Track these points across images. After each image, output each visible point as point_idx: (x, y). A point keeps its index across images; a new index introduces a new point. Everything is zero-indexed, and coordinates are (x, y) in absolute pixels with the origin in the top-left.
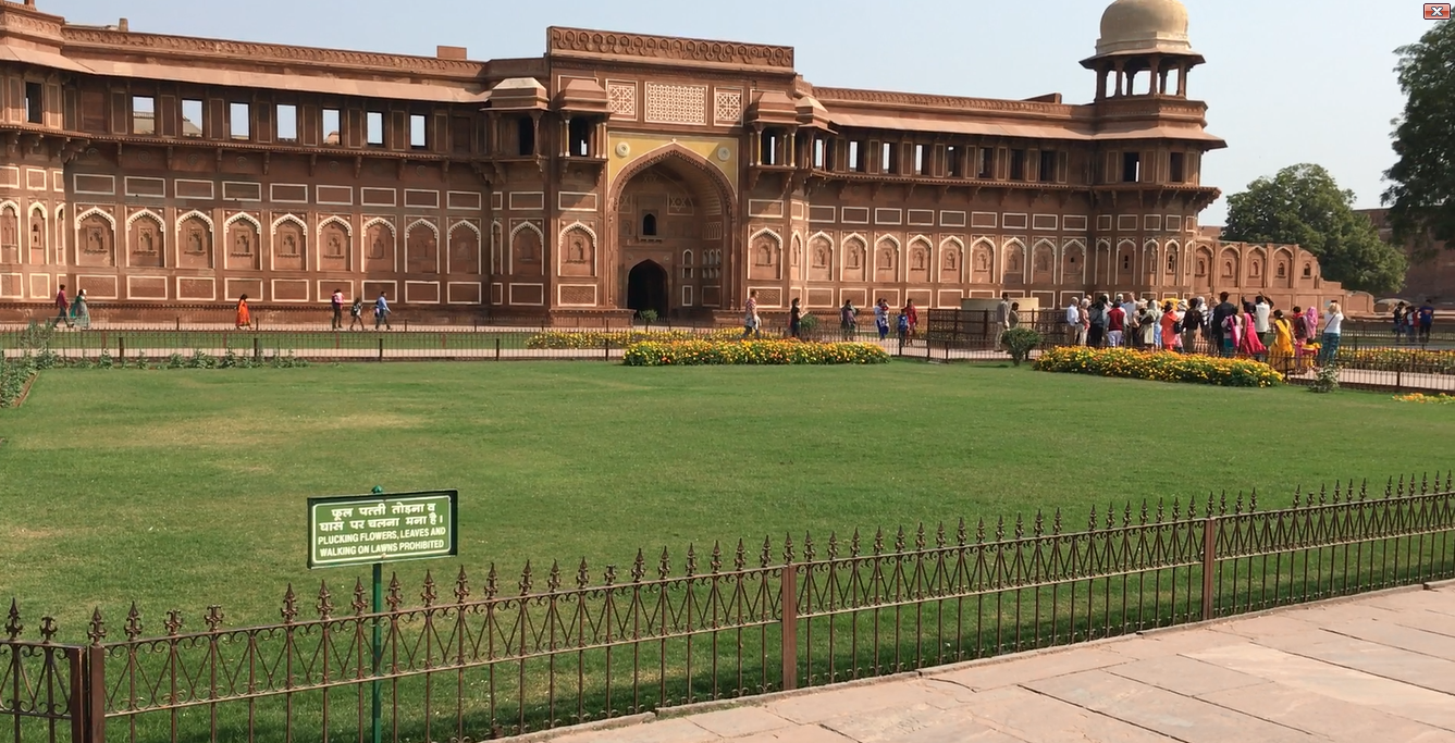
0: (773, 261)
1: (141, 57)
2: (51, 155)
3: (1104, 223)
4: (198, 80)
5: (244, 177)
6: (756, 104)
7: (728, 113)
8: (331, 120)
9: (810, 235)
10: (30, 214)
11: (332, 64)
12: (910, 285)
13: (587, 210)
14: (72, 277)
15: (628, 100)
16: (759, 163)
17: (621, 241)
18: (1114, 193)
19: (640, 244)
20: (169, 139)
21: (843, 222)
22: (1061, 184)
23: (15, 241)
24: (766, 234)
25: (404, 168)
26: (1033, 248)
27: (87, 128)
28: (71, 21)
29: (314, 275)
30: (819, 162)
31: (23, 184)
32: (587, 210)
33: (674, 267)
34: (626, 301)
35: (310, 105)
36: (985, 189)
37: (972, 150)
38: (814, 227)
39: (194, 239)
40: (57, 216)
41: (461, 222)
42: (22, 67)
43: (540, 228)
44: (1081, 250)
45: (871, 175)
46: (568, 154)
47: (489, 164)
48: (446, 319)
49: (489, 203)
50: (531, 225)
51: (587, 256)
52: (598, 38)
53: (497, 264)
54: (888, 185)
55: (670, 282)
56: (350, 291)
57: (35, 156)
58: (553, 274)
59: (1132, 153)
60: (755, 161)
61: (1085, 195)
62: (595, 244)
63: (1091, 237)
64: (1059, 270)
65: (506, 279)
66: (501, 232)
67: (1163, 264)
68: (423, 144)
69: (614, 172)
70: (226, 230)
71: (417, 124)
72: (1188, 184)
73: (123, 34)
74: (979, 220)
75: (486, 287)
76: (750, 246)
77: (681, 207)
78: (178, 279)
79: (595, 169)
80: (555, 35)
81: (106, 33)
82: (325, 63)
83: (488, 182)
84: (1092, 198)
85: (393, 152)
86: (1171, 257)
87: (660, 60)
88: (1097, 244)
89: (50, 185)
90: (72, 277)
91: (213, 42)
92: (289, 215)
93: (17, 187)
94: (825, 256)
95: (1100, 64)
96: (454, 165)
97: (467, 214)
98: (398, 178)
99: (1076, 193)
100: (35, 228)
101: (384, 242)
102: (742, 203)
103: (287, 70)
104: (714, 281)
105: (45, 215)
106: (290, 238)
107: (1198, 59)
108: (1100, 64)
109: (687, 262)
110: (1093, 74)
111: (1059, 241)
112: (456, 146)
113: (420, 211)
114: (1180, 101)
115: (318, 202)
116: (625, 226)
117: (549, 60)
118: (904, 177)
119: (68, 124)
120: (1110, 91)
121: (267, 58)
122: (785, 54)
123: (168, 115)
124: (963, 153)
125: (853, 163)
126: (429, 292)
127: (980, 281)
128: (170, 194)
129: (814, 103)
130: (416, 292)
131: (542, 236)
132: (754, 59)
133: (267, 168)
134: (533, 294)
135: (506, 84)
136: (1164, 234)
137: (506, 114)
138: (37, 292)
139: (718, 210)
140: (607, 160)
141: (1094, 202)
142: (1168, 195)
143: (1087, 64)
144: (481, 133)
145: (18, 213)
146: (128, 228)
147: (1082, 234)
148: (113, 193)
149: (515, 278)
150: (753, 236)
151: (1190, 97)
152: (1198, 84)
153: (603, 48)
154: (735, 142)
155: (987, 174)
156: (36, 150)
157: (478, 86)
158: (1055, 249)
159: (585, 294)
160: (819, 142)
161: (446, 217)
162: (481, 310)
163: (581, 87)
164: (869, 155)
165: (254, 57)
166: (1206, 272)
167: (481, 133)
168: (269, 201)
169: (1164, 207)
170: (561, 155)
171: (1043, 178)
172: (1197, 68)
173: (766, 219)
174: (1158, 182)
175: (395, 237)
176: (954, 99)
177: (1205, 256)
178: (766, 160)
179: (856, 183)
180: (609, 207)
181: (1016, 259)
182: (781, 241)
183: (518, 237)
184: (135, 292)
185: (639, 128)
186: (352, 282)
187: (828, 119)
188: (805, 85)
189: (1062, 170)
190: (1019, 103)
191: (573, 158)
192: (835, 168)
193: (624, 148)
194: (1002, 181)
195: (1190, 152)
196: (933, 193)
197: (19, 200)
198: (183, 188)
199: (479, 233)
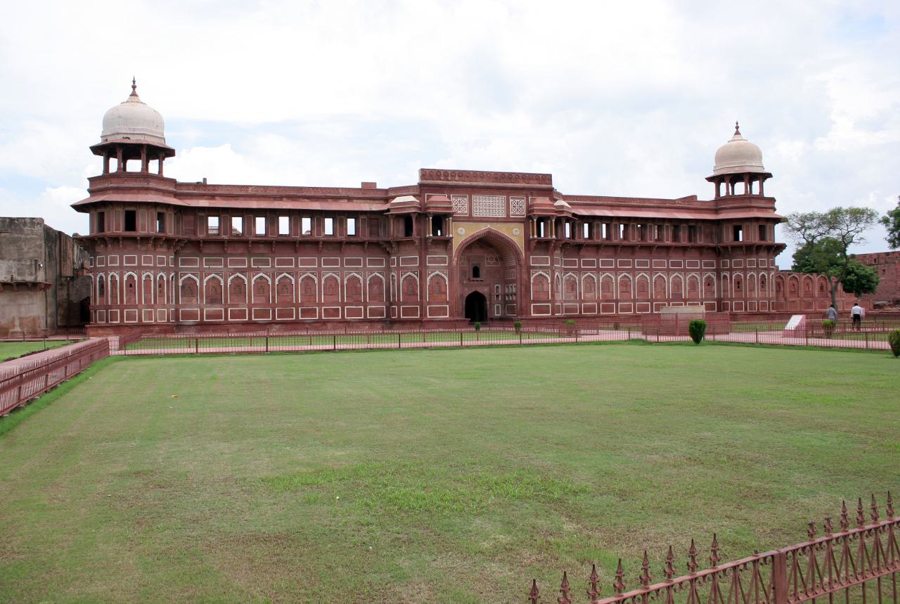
1: (213, 197)
2: (169, 248)
4: (240, 206)
5: (262, 255)
6: (533, 205)
8: (306, 224)
9: (564, 275)
10: (158, 279)
11: (307, 194)
12: (621, 301)
14: (177, 311)
16: (536, 236)
17: (461, 282)
18: (730, 249)
19: (472, 283)
20: (225, 237)
21: (582, 267)
22: (701, 242)
23: (150, 293)
24: (541, 275)
25: (343, 246)
26: (687, 278)
27: (186, 233)
28: (180, 180)
29: (297, 305)
30: (568, 235)
31: (155, 264)
33: (490, 295)
34: (464, 313)
35: (296, 215)
36: (659, 247)
37: (651, 226)
38: (566, 271)
39: (238, 289)
40: (171, 279)
41: (374, 274)
42: (156, 205)
43: (417, 275)
44: (713, 279)
45: (596, 241)
46: (431, 235)
47: (388, 242)
49: (388, 262)
50: (413, 275)
51: (443, 290)
52: (446, 174)
53: (394, 296)
54: (606, 246)
55: (488, 303)
57: (161, 250)
58: (424, 300)
59: (737, 225)
60: (533, 235)
61: (714, 249)
62: (447, 283)
63: (718, 271)
64: (702, 291)
65: (398, 304)
67: (757, 285)
68: (354, 233)
69: (456, 244)
70: (253, 283)
71: (351, 223)
72: (769, 242)
73: (202, 185)
74: (656, 264)
76: (532, 281)
79: (446, 243)
80: (425, 173)
81: (198, 185)
82: (304, 194)
83: (388, 253)
84: (717, 250)
85: (339, 238)
86: (763, 282)
87: (481, 184)
89: (168, 263)
90: (177, 311)
91: (247, 187)
92: (285, 274)
93: (152, 265)
94: (572, 286)
95: (717, 180)
96: (371, 244)
97: (378, 270)
98: (341, 250)
99: (709, 248)
100: (160, 286)
102: (527, 258)
103: (284, 199)
104: (513, 302)
105: (165, 279)
106: (285, 285)
107: (769, 175)
108: (717, 180)
109: (497, 292)
110: (713, 185)
111: (701, 274)
112: (371, 234)
113: (352, 269)
114: (761, 197)
115: (300, 266)
116: (463, 273)
117: (421, 185)
118: (615, 241)
119: (178, 233)
120: (723, 193)
121: (275, 193)
122: (547, 178)
123: (225, 225)
124: (646, 228)
125: (586, 235)
126: (358, 312)
127: (659, 297)
128: (226, 265)
129: (564, 203)
130: (351, 312)
132: (531, 182)
133: (273, 249)
134: (414, 311)
135: (398, 200)
136: (758, 270)
137: (398, 216)
138: (161, 319)
139: (514, 263)
140: (452, 238)
141: (719, 252)
142: (759, 248)
143: (710, 179)
144: (385, 226)
145: (152, 279)
146: (205, 284)
147: (713, 270)
148: (198, 266)
149: (404, 303)
151: (766, 195)
152: (770, 189)
153: (449, 178)
154: (522, 225)
155: (659, 239)
156: (161, 246)
157: (382, 201)
158: (699, 279)
159: (443, 311)
160: (568, 226)
161: (365, 271)
162: (385, 321)
163: (438, 199)
164: (595, 231)
165: (269, 193)
166: (782, 289)
167: (385, 226)
169: (757, 253)
170: (428, 236)
171: (690, 240)
172: (768, 179)
174: (754, 242)
175: (339, 283)
176: (639, 199)
177: (780, 280)
178: (539, 234)
179: (588, 246)
180: (454, 263)
181: (677, 284)
184: (208, 317)
185: (470, 219)
186: (317, 308)
187: (574, 211)
188: (559, 194)
189: (700, 235)
190: (674, 201)
191: (435, 237)
192: (576, 238)
193: (462, 231)
194: (668, 243)
195: (768, 225)
196: (631, 249)
197: (152, 272)
198: (233, 262)
199: (384, 280)
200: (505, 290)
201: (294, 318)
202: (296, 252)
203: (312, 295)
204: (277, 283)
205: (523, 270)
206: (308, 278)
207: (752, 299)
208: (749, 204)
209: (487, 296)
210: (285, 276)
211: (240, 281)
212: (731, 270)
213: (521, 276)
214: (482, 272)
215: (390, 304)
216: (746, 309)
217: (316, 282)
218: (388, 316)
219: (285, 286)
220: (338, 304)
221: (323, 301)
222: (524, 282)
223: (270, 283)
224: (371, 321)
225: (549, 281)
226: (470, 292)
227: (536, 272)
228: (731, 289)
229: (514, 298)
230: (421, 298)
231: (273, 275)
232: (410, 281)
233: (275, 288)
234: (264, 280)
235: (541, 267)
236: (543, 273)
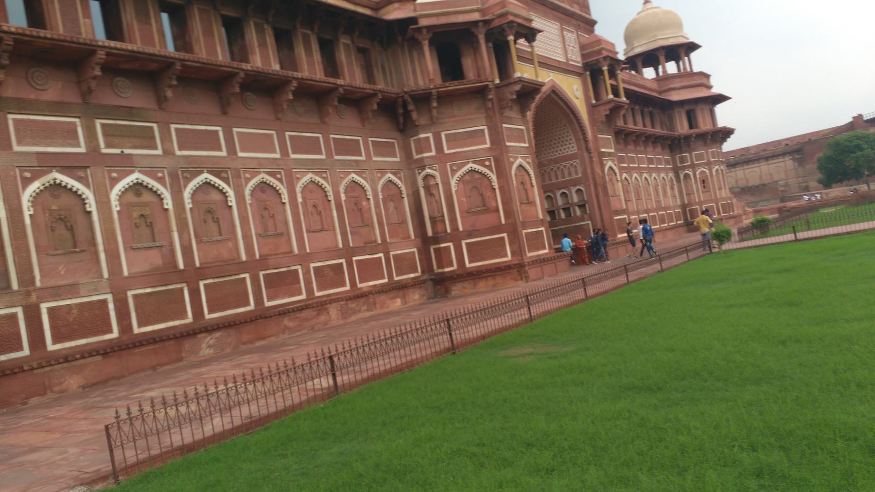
3: (683, 160)
5: (130, 113)
29: (253, 266)
39: (61, 230)
43: (489, 167)
48: (398, 302)
50: (475, 166)
56: (299, 282)
63: (676, 171)
65: (456, 237)
66: (439, 180)
75: (424, 253)
78: (44, 307)
88: (681, 176)
92: (205, 176)
101: (320, 208)
106: (209, 211)
131: (494, 177)
133: (169, 93)
139: (572, 148)
141: (675, 145)
144: (383, 68)
149: (470, 235)
162: (424, 282)
167: (383, 68)
168: (174, 154)
183: (461, 185)
198: (26, 132)
201: (252, 307)
202: (224, 113)
203: (281, 234)
204: (188, 205)
205: (594, 159)
206: (264, 186)
207: (723, 199)
208: (699, 82)
210: (208, 184)
211: (66, 200)
212: (693, 166)
213: (592, 169)
215: (425, 242)
216: (719, 213)
217: (285, 198)
218: (423, 272)
219: (211, 210)
220: (336, 252)
221: (308, 251)
222: (599, 181)
223: (168, 203)
224: (401, 288)
228: (698, 190)
229: (578, 212)
230: (508, 213)
231: (174, 176)
232: (474, 181)
233: (186, 219)
234: (146, 197)
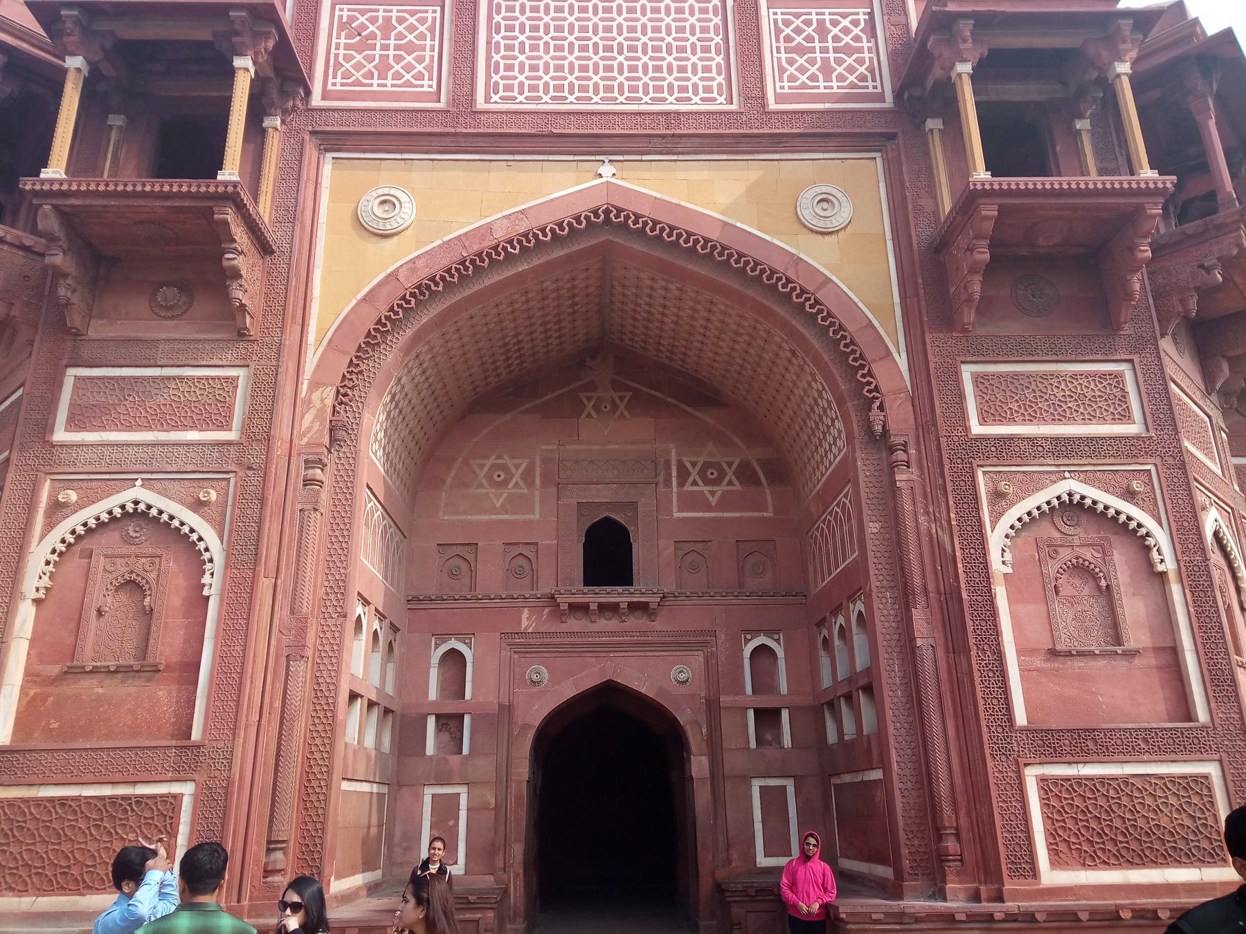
0: (1137, 636)
7: (826, 70)
13: (193, 436)
15: (410, 48)
16: (981, 174)
19: (574, 624)
24: (1073, 508)
32: (193, 436)
55: (699, 765)
62: (213, 584)
77: (719, 490)
109: (763, 682)
150: (1012, 516)
154: (869, 171)
173: (1056, 439)
182: (1160, 537)
200: (815, 674)
209: (684, 717)
213: (893, 521)
214: (651, 555)
225: (1169, 565)
226: (568, 691)
227: (1032, 484)
235: (1063, 447)
236: (1093, 493)
